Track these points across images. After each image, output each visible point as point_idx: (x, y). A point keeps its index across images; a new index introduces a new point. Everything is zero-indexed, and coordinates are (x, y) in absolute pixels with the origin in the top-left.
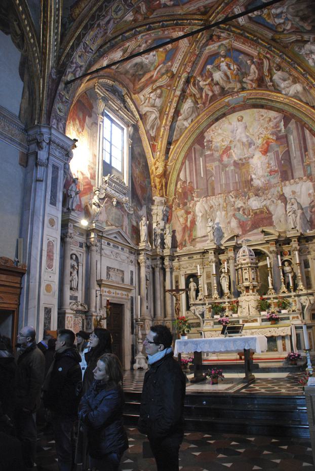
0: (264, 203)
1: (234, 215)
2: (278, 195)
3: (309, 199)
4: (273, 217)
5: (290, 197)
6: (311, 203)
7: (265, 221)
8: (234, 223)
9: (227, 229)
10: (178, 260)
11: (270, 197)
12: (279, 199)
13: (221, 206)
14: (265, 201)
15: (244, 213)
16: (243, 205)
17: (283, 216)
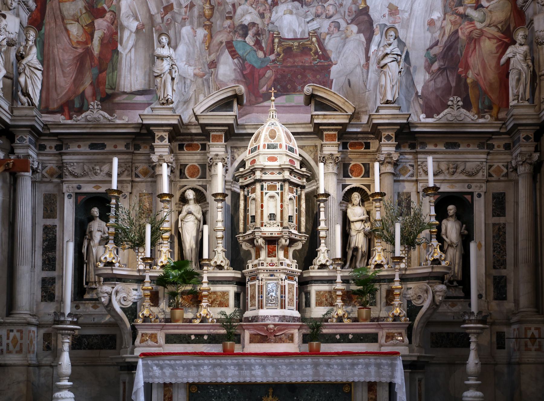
0: (314, 25)
1: (230, 46)
2: (354, 8)
3: (429, 34)
4: (334, 69)
5: (383, 21)
6: (431, 48)
7: (309, 76)
8: (227, 68)
9: (207, 80)
10: (59, 148)
11: (331, 10)
12: (353, 21)
13: (196, 11)
14: (318, 20)
15: (258, 43)
16: (258, 21)
17: (358, 70)
